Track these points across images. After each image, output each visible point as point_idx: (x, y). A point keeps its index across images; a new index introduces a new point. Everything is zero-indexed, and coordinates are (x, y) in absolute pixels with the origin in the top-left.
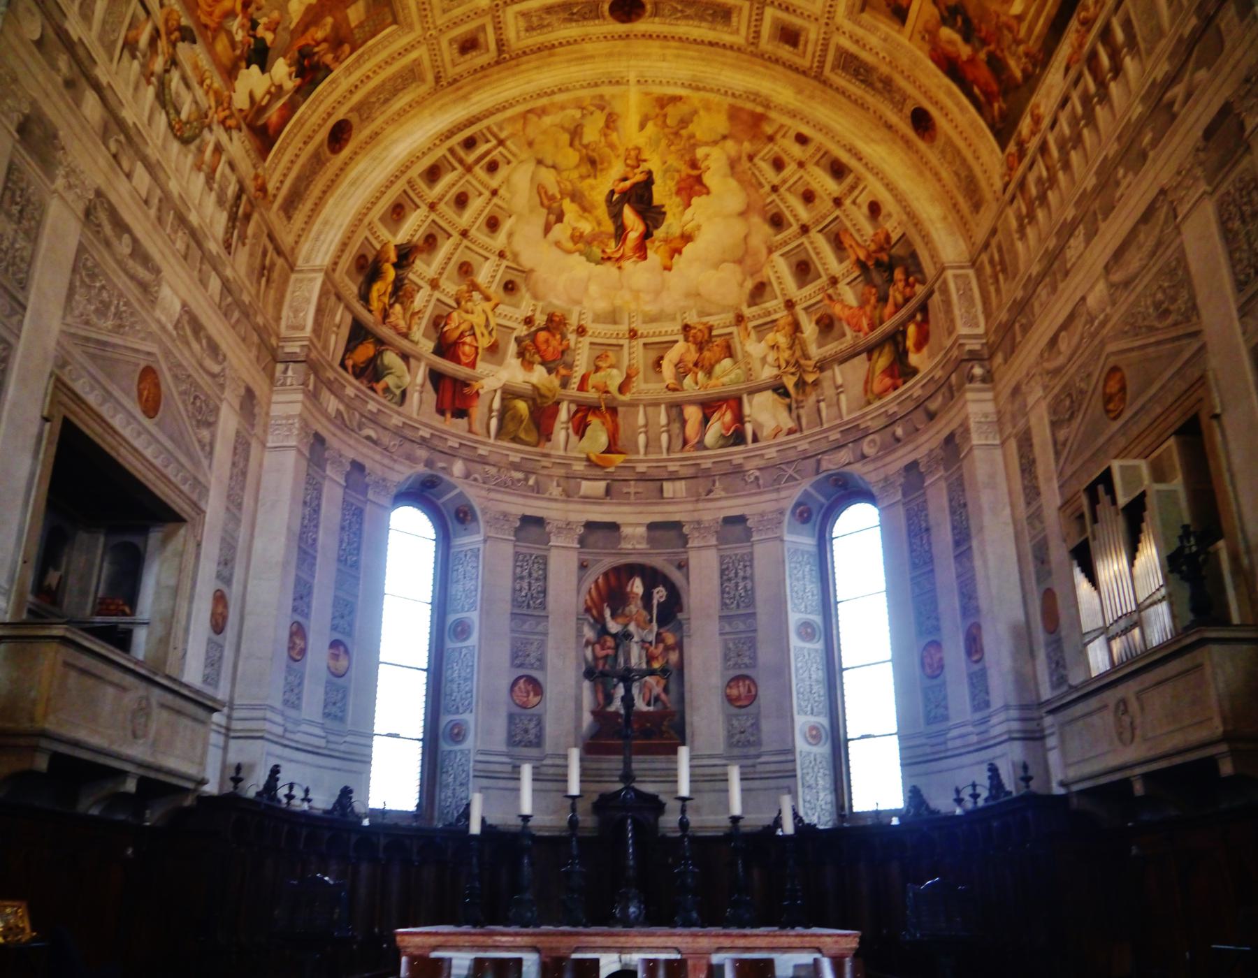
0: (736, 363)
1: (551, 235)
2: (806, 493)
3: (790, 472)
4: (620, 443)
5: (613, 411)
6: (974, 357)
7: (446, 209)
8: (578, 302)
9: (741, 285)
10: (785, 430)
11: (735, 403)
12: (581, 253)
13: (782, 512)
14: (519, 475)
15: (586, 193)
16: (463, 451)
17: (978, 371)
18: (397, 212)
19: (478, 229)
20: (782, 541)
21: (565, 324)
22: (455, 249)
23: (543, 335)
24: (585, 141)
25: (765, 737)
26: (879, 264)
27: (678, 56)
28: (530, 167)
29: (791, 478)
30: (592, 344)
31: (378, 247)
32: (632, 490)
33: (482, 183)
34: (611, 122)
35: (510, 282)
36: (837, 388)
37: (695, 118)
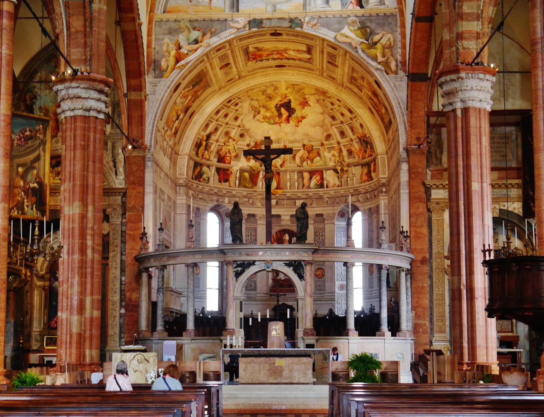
0: (321, 158)
1: (256, 118)
2: (342, 208)
3: (338, 200)
4: (281, 186)
5: (278, 174)
6: (384, 185)
7: (222, 120)
9: (323, 134)
10: (337, 185)
11: (320, 172)
12: (266, 122)
13: (334, 214)
14: (246, 200)
16: (228, 194)
17: (384, 190)
18: (207, 126)
24: (267, 93)
25: (327, 288)
26: (364, 140)
27: (298, 74)
29: (338, 203)
31: (201, 138)
32: (285, 203)
34: (276, 88)
35: (242, 134)
36: (353, 174)
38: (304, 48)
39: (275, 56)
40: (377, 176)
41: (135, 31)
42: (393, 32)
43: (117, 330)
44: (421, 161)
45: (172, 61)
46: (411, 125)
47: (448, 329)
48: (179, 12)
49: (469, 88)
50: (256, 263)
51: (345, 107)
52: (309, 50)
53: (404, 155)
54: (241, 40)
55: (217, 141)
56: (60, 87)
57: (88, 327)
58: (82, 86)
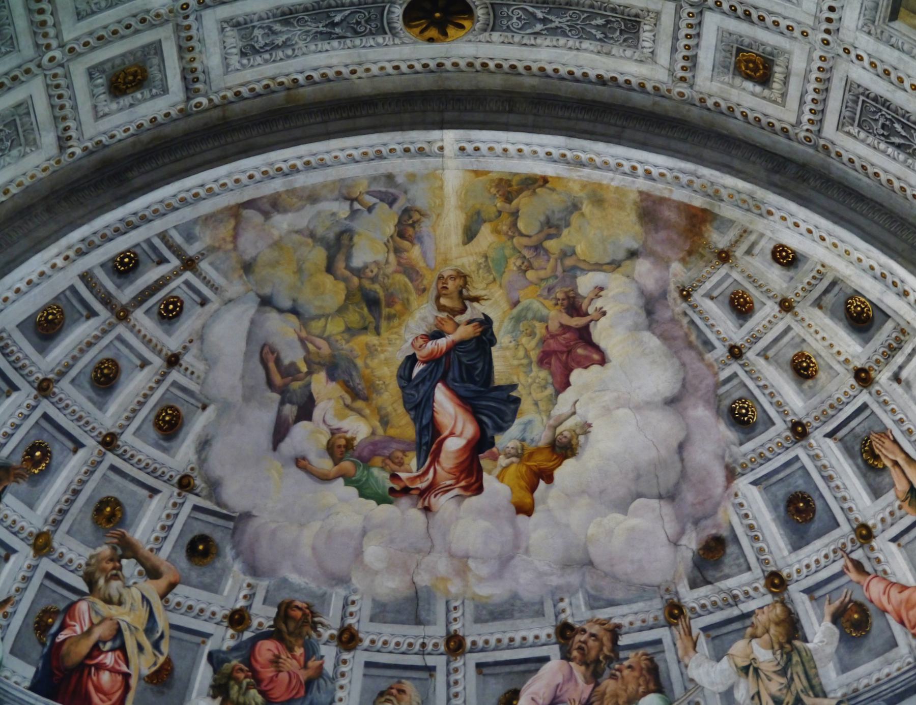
1: (286, 446)
8: (342, 580)
9: (675, 543)
12: (349, 481)
15: (359, 362)
19: (136, 433)
21: (314, 626)
22: (90, 473)
23: (267, 649)
28: (248, 309)
30: (368, 665)
33: (147, 342)
35: (203, 539)
37: (575, 219)
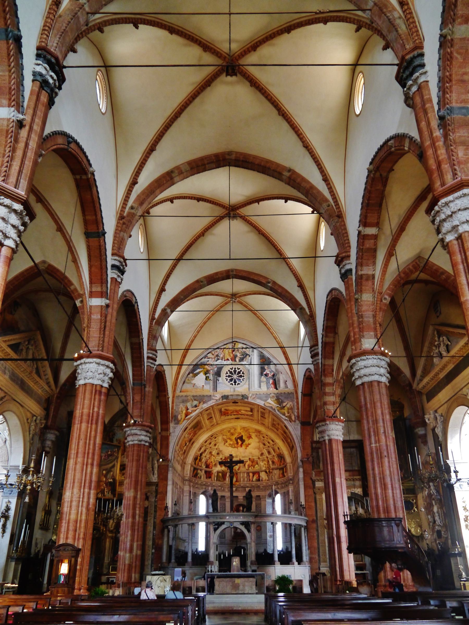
5: (237, 474)
6: (291, 479)
7: (208, 445)
11: (258, 473)
14: (220, 488)
17: (291, 482)
18: (200, 449)
20: (266, 501)
34: (235, 429)
38: (249, 409)
39: (235, 413)
40: (288, 474)
41: (166, 401)
42: (292, 401)
43: (150, 562)
44: (309, 467)
45: (183, 416)
46: (304, 448)
47: (328, 560)
48: (187, 392)
49: (331, 429)
50: (225, 523)
51: (270, 439)
52: (252, 410)
53: (301, 464)
54: (218, 405)
55: (205, 457)
56: (127, 429)
57: (134, 560)
58: (138, 429)
